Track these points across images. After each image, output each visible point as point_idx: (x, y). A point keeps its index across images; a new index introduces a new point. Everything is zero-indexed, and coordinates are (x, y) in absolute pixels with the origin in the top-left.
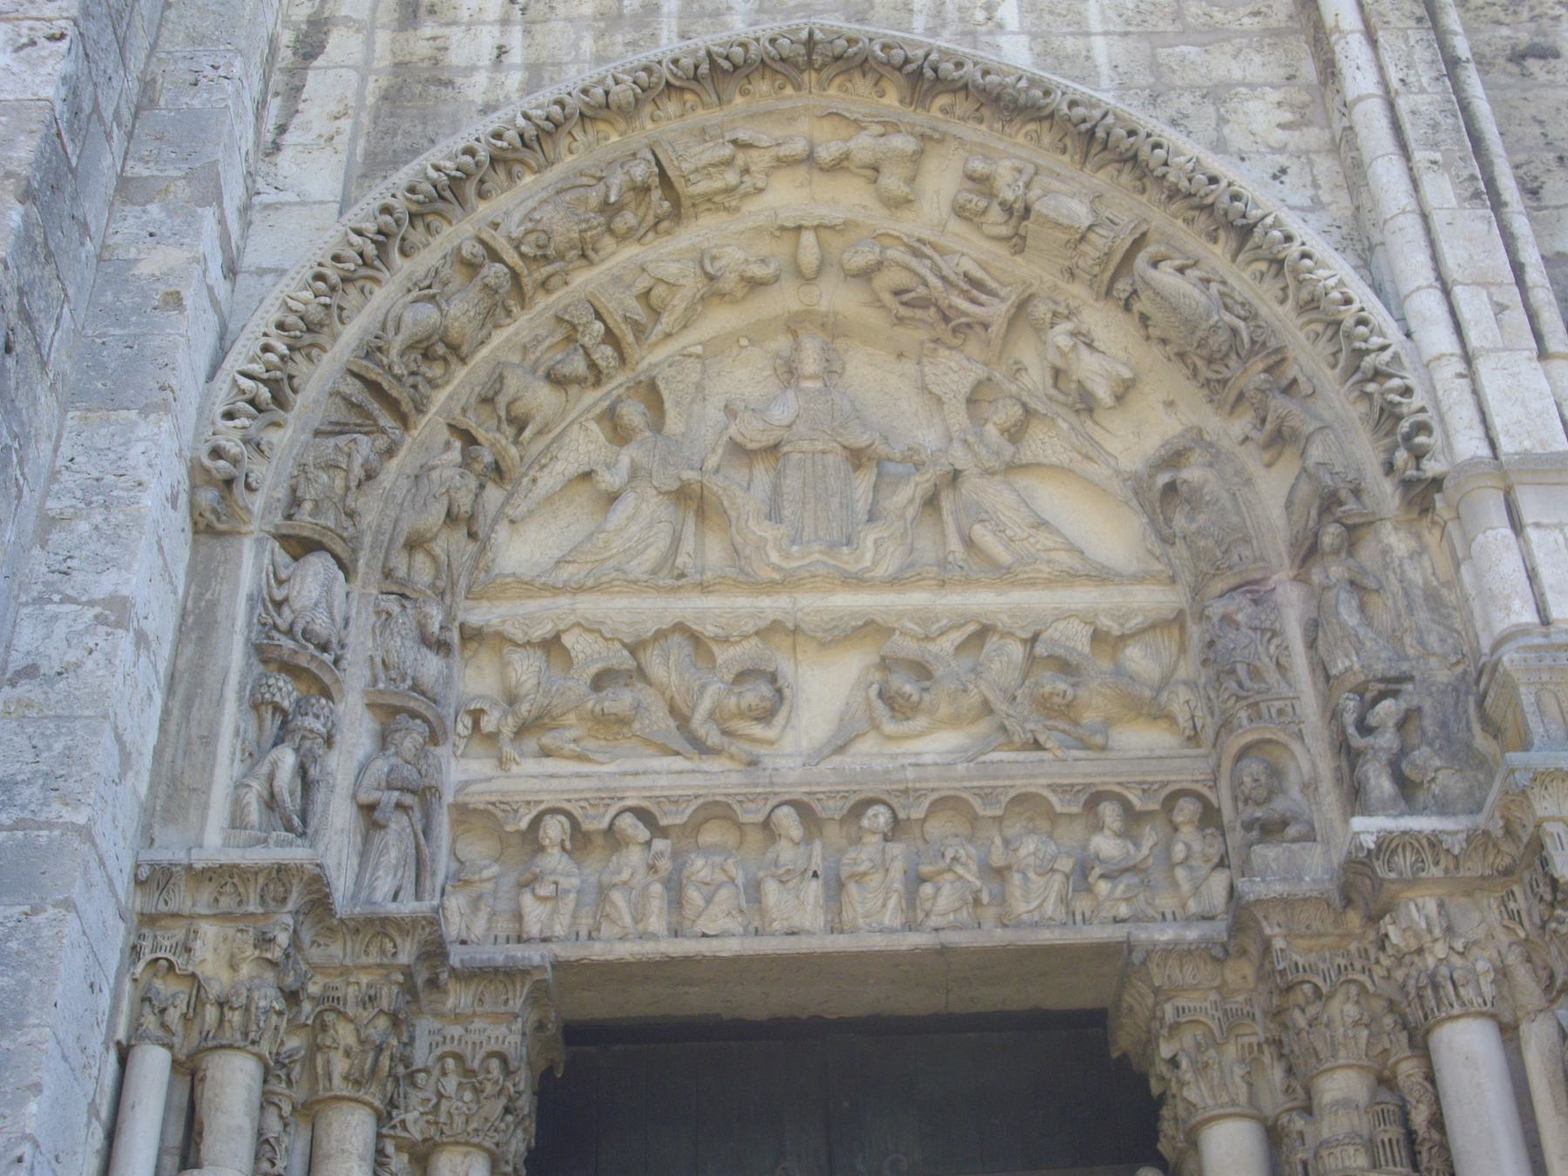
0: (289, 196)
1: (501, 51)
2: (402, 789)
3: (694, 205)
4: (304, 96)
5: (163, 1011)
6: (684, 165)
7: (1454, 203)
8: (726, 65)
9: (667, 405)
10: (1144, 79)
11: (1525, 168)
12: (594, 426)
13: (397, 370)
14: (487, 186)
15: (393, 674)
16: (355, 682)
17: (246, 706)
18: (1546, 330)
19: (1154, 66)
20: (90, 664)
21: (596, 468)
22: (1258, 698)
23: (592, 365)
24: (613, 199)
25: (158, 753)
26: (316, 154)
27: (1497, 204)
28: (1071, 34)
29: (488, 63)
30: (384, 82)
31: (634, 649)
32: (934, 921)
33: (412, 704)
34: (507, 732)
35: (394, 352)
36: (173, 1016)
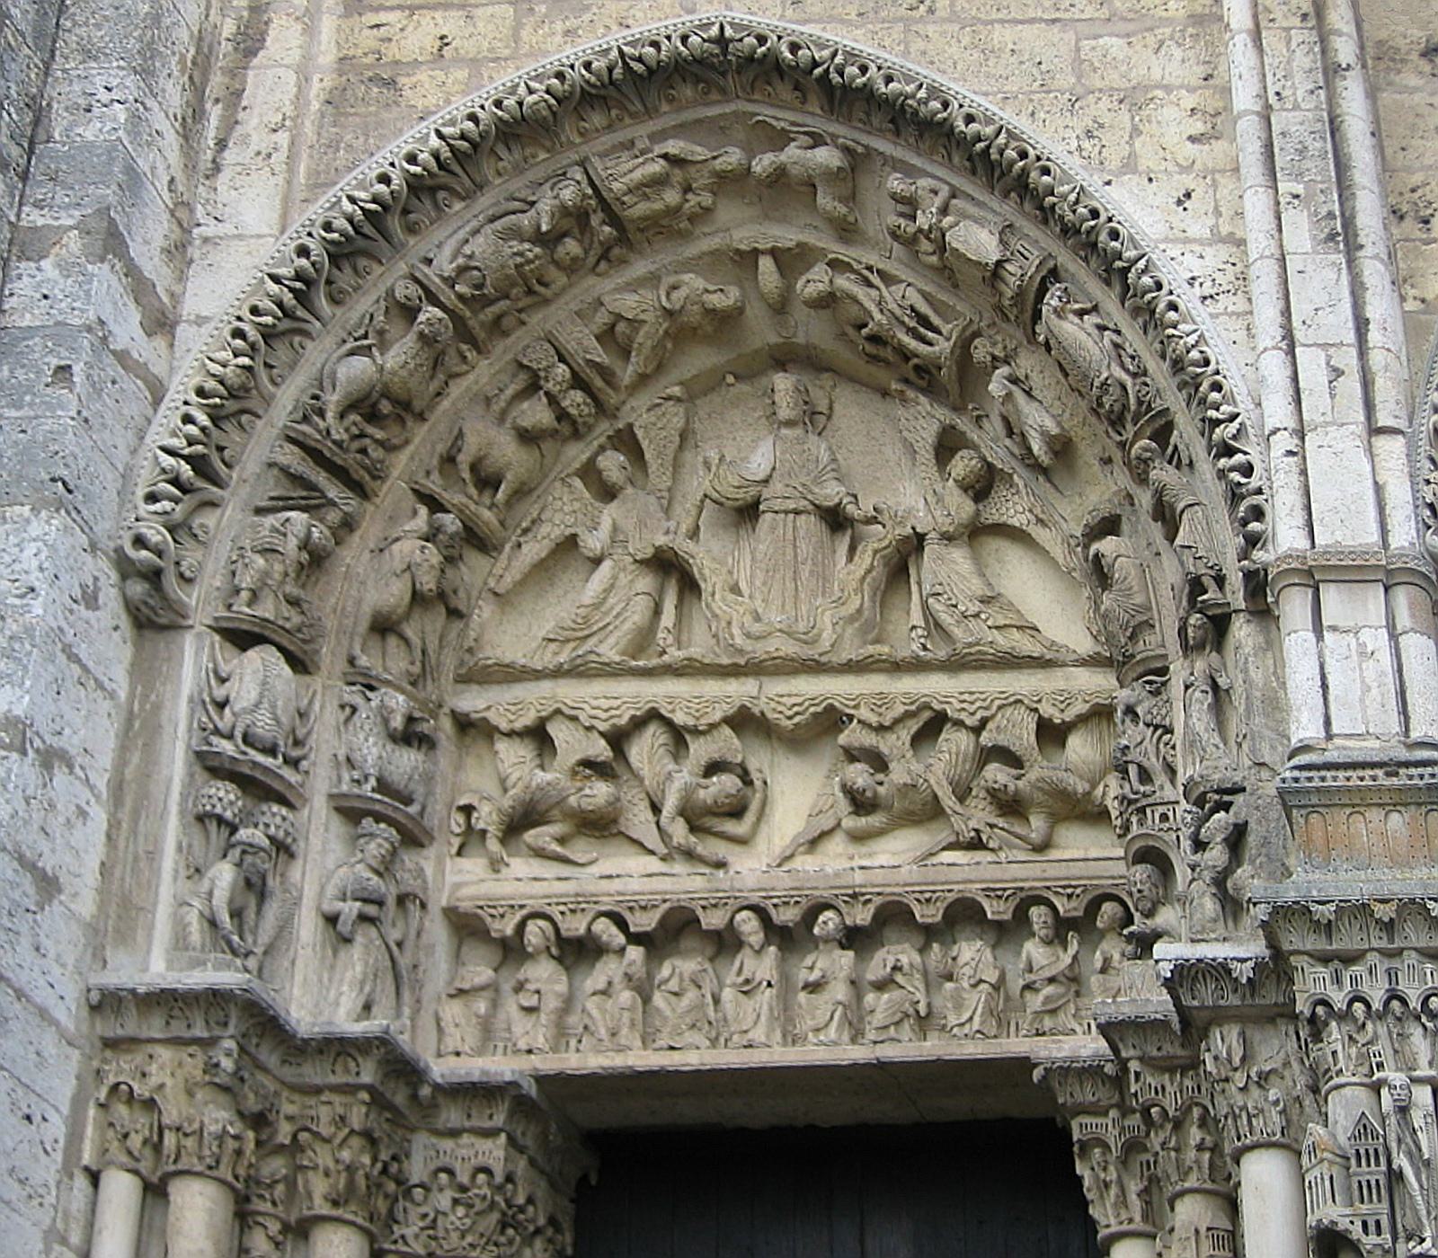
0: (227, 228)
2: (365, 901)
4: (244, 103)
6: (616, 186)
15: (356, 774)
24: (544, 228)
33: (377, 807)
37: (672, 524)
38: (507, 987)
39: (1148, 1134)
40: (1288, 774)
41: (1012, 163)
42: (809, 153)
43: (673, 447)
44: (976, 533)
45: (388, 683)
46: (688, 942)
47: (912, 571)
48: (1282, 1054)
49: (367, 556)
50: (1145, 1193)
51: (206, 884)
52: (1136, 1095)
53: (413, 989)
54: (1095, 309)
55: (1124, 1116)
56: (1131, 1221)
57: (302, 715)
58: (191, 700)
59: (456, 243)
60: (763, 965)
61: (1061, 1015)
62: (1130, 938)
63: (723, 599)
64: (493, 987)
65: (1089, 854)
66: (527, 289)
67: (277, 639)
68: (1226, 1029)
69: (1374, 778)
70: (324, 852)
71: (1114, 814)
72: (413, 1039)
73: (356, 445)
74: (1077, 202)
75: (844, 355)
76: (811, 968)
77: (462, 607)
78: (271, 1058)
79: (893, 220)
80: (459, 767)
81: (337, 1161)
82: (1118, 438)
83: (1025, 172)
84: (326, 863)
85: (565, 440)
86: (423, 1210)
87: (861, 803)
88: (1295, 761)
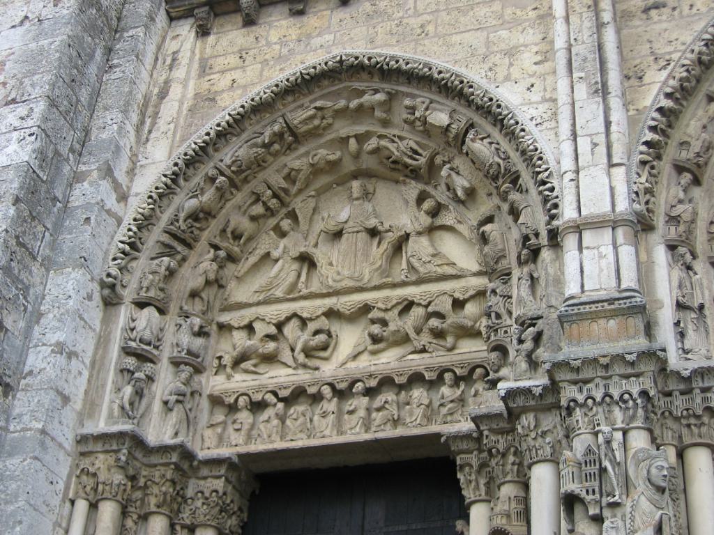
0: (150, 161)
2: (179, 395)
3: (303, 136)
6: (295, 122)
7: (585, 97)
9: (300, 219)
12: (272, 233)
13: (182, 228)
14: (217, 146)
15: (179, 349)
16: (166, 353)
17: (118, 371)
20: (48, 369)
21: (271, 250)
22: (497, 327)
23: (268, 209)
24: (266, 141)
25: (86, 392)
33: (186, 360)
34: (229, 364)
36: (88, 488)
37: (307, 243)
38: (229, 422)
39: (490, 460)
40: (563, 309)
41: (456, 86)
42: (373, 97)
43: (310, 214)
44: (431, 230)
45: (194, 315)
46: (302, 399)
47: (404, 248)
48: (553, 423)
49: (190, 269)
50: (488, 484)
51: (121, 394)
52: (486, 444)
53: (194, 426)
54: (489, 136)
55: (480, 453)
56: (480, 495)
57: (161, 330)
58: (122, 329)
59: (230, 154)
60: (330, 405)
61: (455, 415)
62: (487, 382)
63: (326, 268)
64: (224, 423)
65: (472, 350)
66: (259, 164)
67: (154, 303)
68: (528, 415)
69: (603, 307)
70: (165, 378)
71: (484, 333)
72: (192, 444)
73: (190, 230)
74: (484, 96)
75: (381, 170)
76: (351, 405)
77: (224, 283)
78: (139, 455)
79: (405, 116)
80: (218, 342)
81: (160, 491)
82: (495, 185)
83: (462, 89)
84: (166, 381)
85: (268, 218)
86: (190, 507)
87: (375, 339)
88: (567, 303)
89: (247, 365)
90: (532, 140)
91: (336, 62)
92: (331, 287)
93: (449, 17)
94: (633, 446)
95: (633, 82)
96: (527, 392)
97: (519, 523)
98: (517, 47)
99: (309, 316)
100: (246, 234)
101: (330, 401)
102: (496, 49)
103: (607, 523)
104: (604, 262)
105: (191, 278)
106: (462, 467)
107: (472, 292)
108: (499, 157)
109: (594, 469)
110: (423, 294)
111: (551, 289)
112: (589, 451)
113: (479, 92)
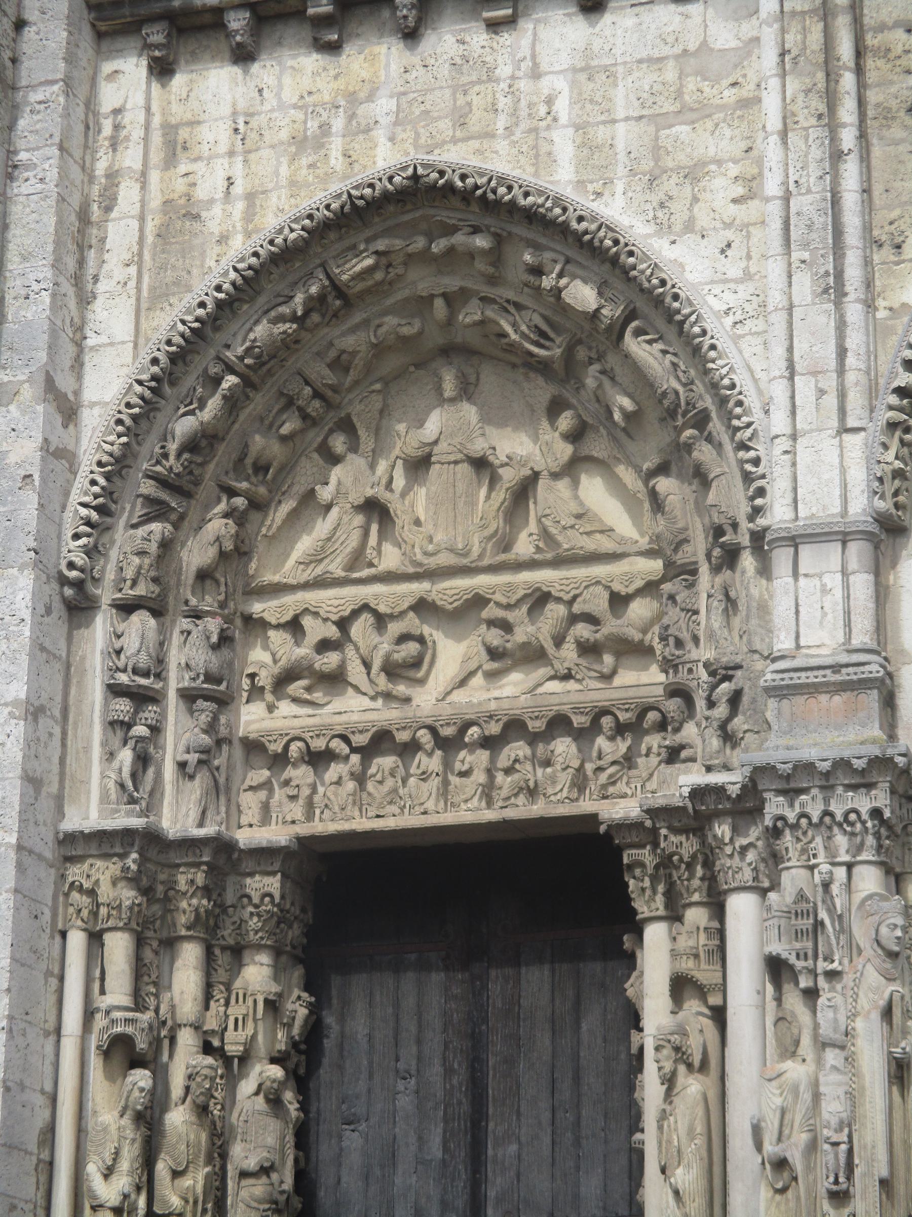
1: (230, 181)
4: (107, 247)
5: (80, 911)
7: (809, 299)
8: (360, 203)
9: (360, 432)
10: (647, 164)
11: (896, 224)
12: (315, 456)
18: (849, 407)
19: (657, 151)
20: (9, 745)
22: (677, 661)
26: (117, 299)
27: (841, 294)
28: (604, 123)
29: (222, 195)
30: (157, 222)
31: (343, 624)
32: (500, 804)
35: (172, 458)
73: (187, 471)
89: (296, 688)
90: (727, 369)
91: (407, 178)
92: (420, 565)
93: (591, 85)
94: (860, 888)
95: (886, 253)
96: (719, 791)
97: (711, 967)
98: (705, 164)
99: (389, 611)
100: (275, 464)
101: (430, 754)
102: (670, 164)
103: (822, 1001)
104: (828, 601)
105: (196, 554)
106: (630, 867)
107: (639, 583)
108: (678, 378)
109: (807, 923)
110: (564, 581)
111: (754, 622)
112: (801, 897)
113: (645, 266)
